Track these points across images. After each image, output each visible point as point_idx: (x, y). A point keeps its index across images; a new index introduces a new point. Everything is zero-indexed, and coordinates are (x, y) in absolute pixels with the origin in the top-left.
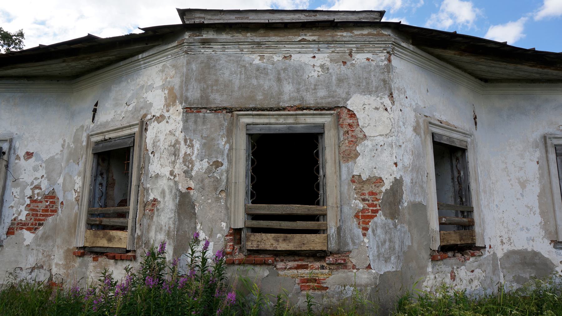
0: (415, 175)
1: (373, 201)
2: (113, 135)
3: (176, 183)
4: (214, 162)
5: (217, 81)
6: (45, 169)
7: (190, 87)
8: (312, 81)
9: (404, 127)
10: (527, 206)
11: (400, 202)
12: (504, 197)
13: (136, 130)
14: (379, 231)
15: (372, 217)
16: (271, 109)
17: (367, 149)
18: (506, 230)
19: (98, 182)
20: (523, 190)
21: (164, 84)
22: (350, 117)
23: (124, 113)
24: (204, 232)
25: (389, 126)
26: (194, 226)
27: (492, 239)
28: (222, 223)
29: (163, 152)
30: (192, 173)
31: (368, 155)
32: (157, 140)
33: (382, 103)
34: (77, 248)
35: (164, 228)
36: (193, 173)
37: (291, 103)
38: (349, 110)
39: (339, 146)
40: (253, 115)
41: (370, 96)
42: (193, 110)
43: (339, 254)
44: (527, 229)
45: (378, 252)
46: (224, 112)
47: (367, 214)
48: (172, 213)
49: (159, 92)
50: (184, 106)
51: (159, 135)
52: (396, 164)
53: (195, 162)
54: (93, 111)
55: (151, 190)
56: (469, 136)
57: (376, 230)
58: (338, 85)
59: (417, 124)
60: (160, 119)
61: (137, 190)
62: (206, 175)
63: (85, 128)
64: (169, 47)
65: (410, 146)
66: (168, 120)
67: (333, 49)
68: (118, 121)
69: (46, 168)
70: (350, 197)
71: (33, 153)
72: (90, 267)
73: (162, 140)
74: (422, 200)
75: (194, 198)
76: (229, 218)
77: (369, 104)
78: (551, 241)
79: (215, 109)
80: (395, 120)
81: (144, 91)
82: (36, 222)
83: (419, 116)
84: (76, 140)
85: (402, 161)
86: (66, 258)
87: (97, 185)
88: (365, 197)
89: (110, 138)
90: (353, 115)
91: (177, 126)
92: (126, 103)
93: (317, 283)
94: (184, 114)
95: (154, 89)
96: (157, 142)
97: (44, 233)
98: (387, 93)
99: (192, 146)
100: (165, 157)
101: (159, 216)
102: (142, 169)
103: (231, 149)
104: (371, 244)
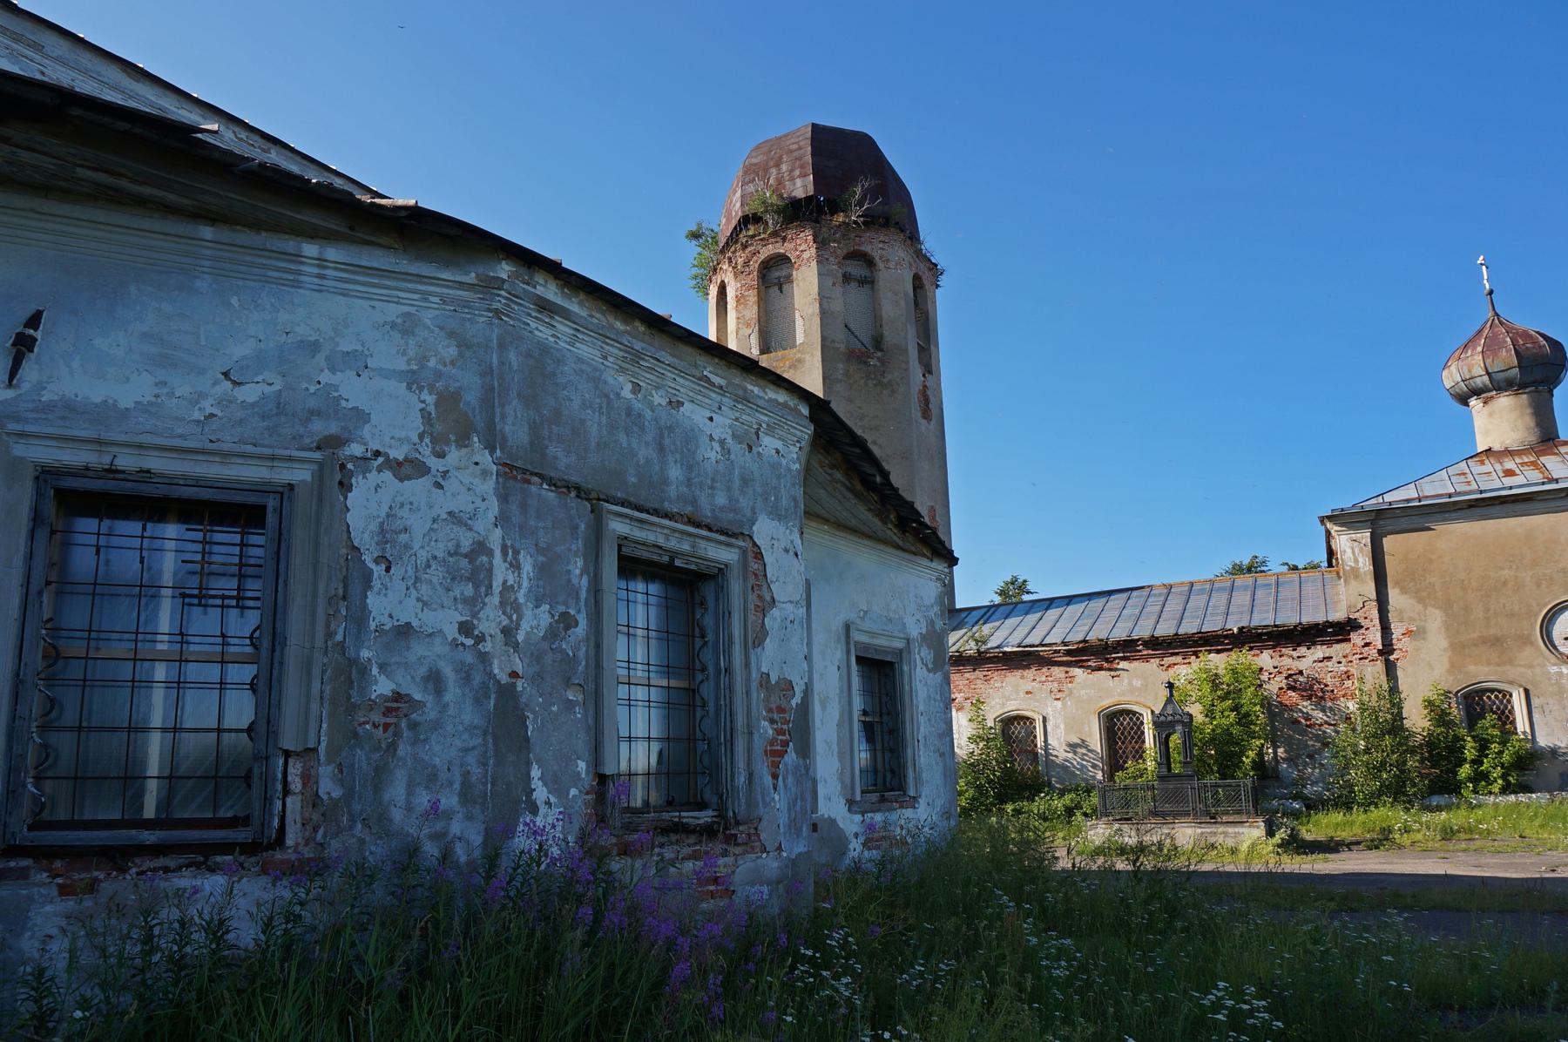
2: (157, 463)
3: (484, 658)
5: (557, 413)
7: (509, 410)
23: (211, 401)
24: (545, 784)
28: (579, 762)
29: (428, 566)
35: (443, 776)
36: (520, 637)
38: (755, 544)
40: (631, 518)
51: (404, 512)
53: (524, 608)
55: (382, 667)
60: (407, 469)
62: (546, 645)
64: (443, 276)
67: (737, 414)
94: (500, 480)
95: (365, 374)
99: (516, 566)
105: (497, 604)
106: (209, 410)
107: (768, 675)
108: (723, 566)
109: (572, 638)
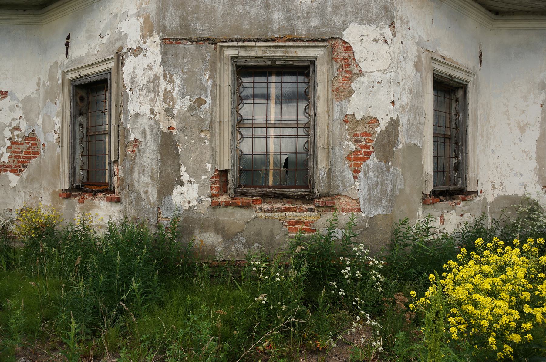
0: (412, 116)
1: (366, 142)
2: (88, 71)
3: (157, 122)
4: (197, 99)
5: (197, 7)
6: (22, 109)
7: (168, 14)
8: (305, 7)
9: (404, 62)
10: (524, 152)
11: (395, 143)
12: (501, 142)
13: (112, 64)
14: (371, 174)
15: (364, 160)
16: (258, 40)
17: (363, 86)
18: (499, 175)
19: (77, 123)
20: (522, 134)
21: (138, 12)
22: (345, 50)
23: (98, 46)
24: (188, 173)
25: (387, 60)
26: (178, 167)
27: (484, 184)
29: (142, 89)
30: (174, 112)
31: (363, 93)
32: (135, 76)
33: (381, 34)
34: (63, 190)
35: (147, 169)
36: (175, 112)
37: (281, 34)
38: (345, 42)
39: (333, 83)
41: (369, 26)
42: (171, 41)
43: (328, 196)
44: (521, 175)
45: (369, 195)
46: (207, 43)
47: (360, 156)
48: (154, 154)
49: (134, 20)
50: (162, 36)
51: (136, 70)
52: (393, 103)
54: (65, 45)
55: (132, 129)
56: (472, 76)
57: (368, 173)
58: (334, 13)
59: (418, 59)
60: (137, 52)
61: (117, 131)
62: (189, 114)
63: (59, 64)
65: (409, 83)
66: (145, 53)
68: (92, 55)
69: (23, 108)
70: (342, 138)
71: (7, 92)
72: (77, 209)
73: (140, 76)
74: (418, 143)
75: (177, 138)
76: (214, 160)
77: (367, 36)
78: (544, 187)
79: (196, 40)
80: (395, 54)
81: (118, 20)
82: (20, 164)
83: (422, 51)
84: (52, 77)
85: (399, 100)
86: (53, 199)
87: (77, 127)
88: (358, 138)
89: (86, 75)
90: (349, 48)
91: (155, 59)
92: (100, 35)
93: (305, 226)
95: (128, 18)
96: (135, 78)
97: (29, 176)
98: (389, 22)
99: (172, 82)
100: (144, 94)
101: (140, 157)
102: (122, 106)
103: (214, 85)
104: (362, 187)
105: (162, 99)
107: (354, 115)
108: (314, 59)
109: (202, 109)
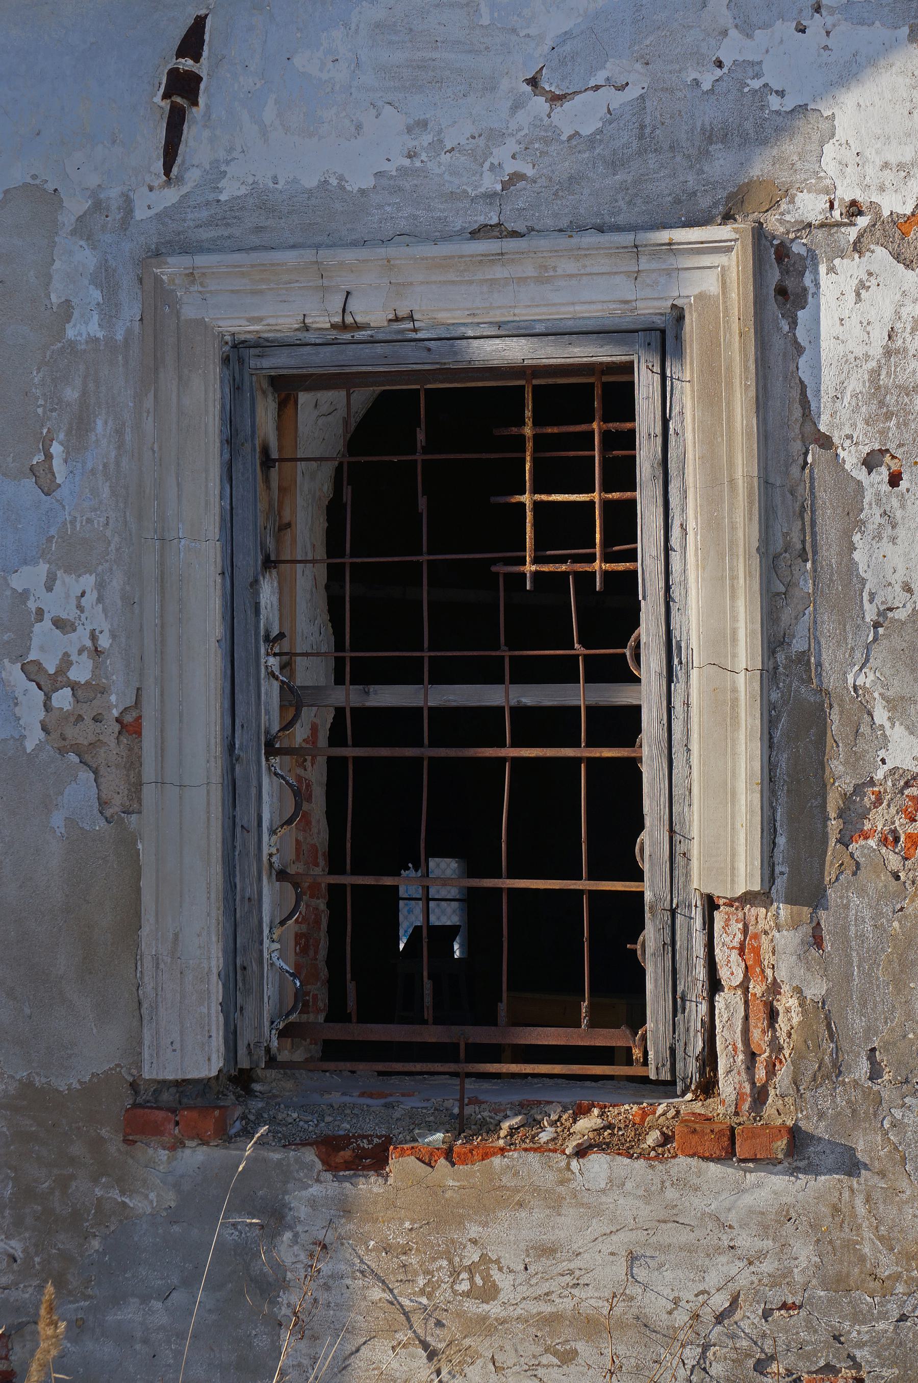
23: (512, 146)
55: (895, 705)
106: (511, 167)
